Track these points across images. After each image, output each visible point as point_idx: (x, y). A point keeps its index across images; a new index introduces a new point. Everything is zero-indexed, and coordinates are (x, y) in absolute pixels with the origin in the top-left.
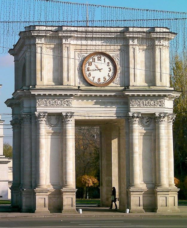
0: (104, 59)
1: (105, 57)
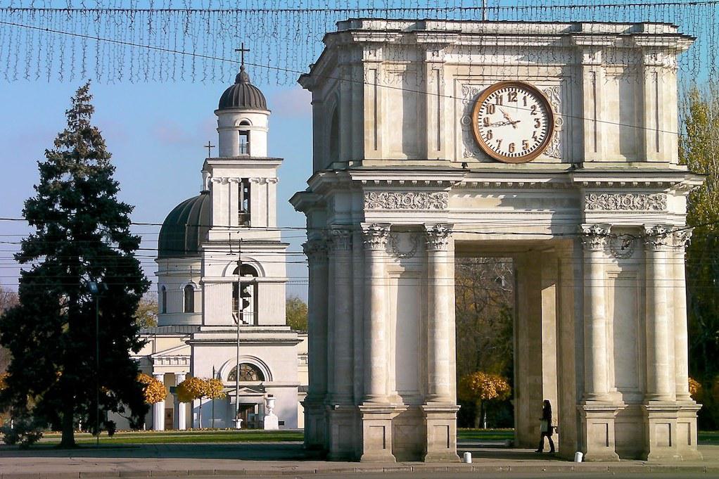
0: (525, 98)
1: (527, 94)
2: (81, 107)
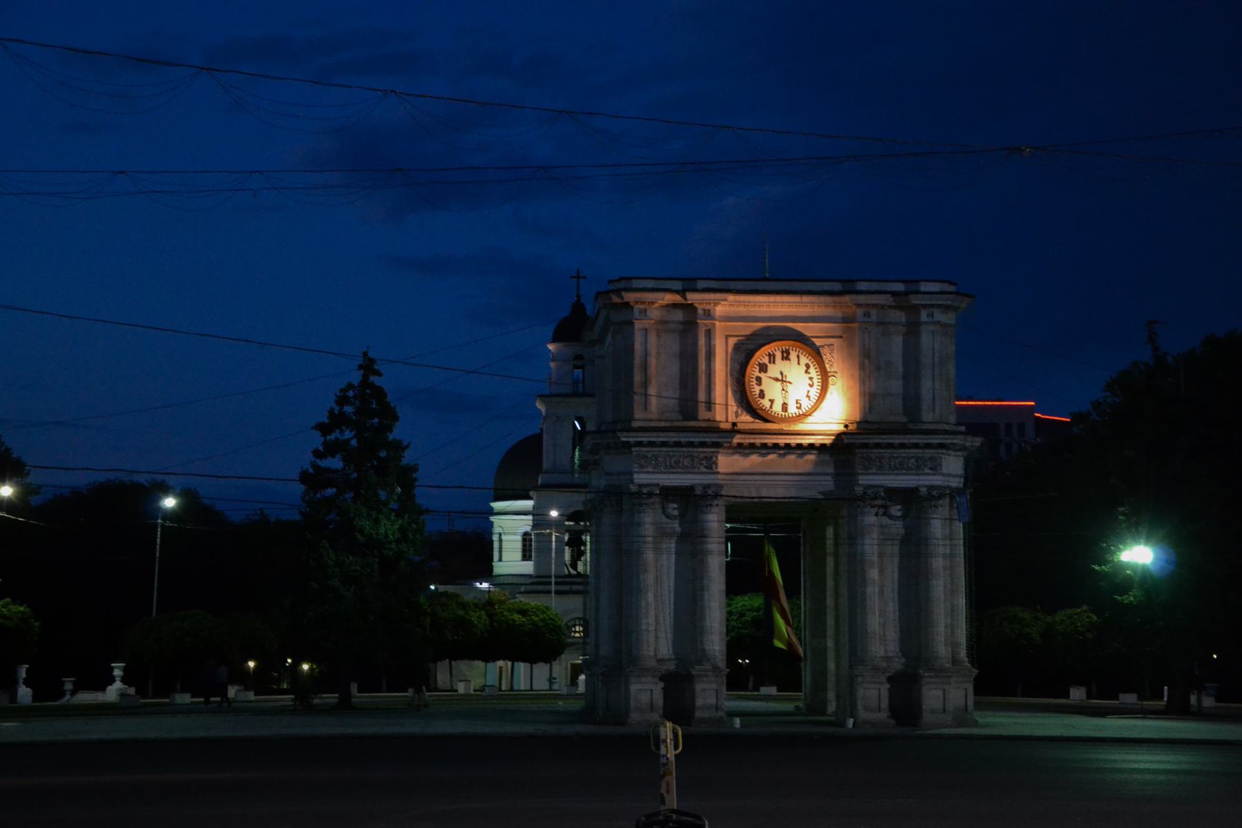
0: (798, 357)
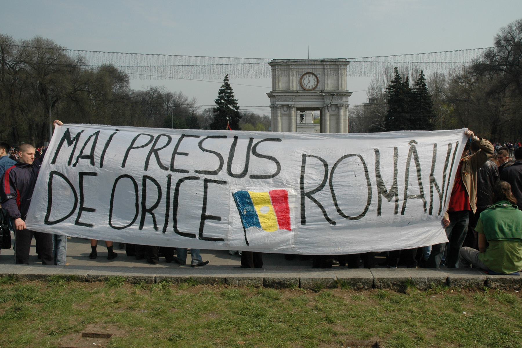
2: (226, 79)
